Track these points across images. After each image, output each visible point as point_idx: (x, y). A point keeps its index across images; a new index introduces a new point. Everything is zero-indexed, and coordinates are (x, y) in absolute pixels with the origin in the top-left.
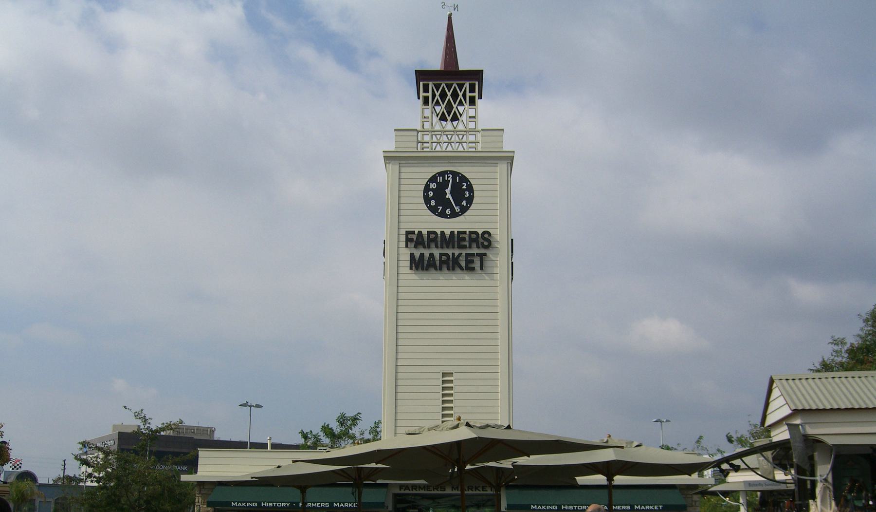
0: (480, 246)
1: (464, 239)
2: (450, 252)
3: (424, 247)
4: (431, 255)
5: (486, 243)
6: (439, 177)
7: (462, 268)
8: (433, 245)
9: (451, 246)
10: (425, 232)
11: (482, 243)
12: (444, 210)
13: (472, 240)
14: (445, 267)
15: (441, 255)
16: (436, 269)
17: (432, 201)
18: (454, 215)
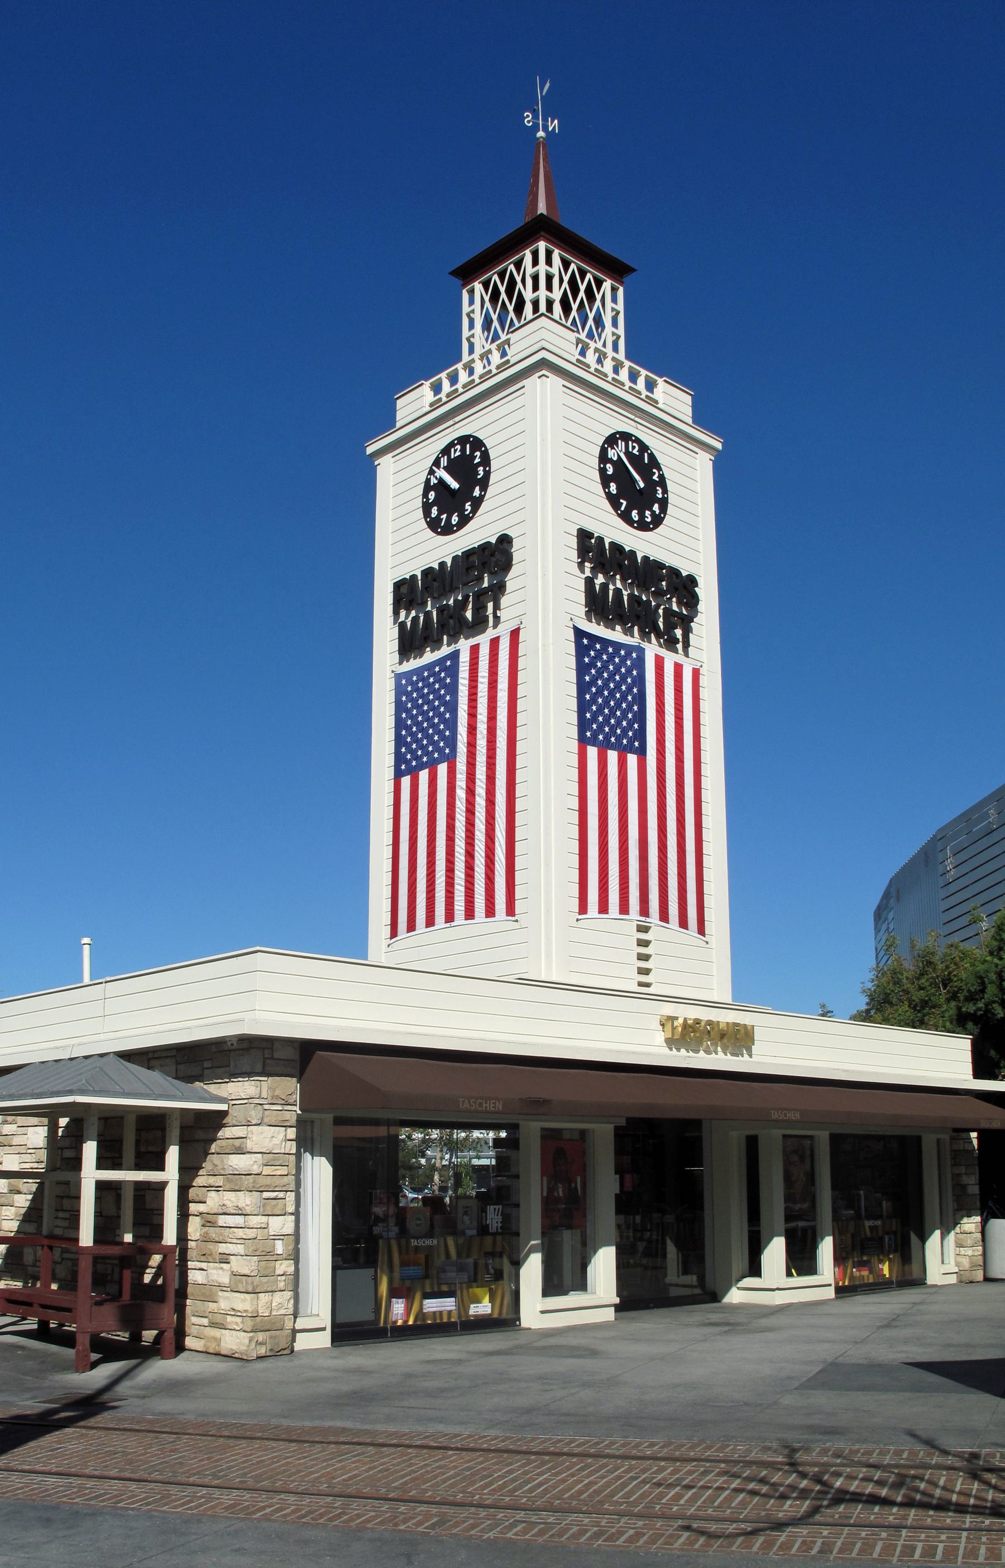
6: (442, 459)
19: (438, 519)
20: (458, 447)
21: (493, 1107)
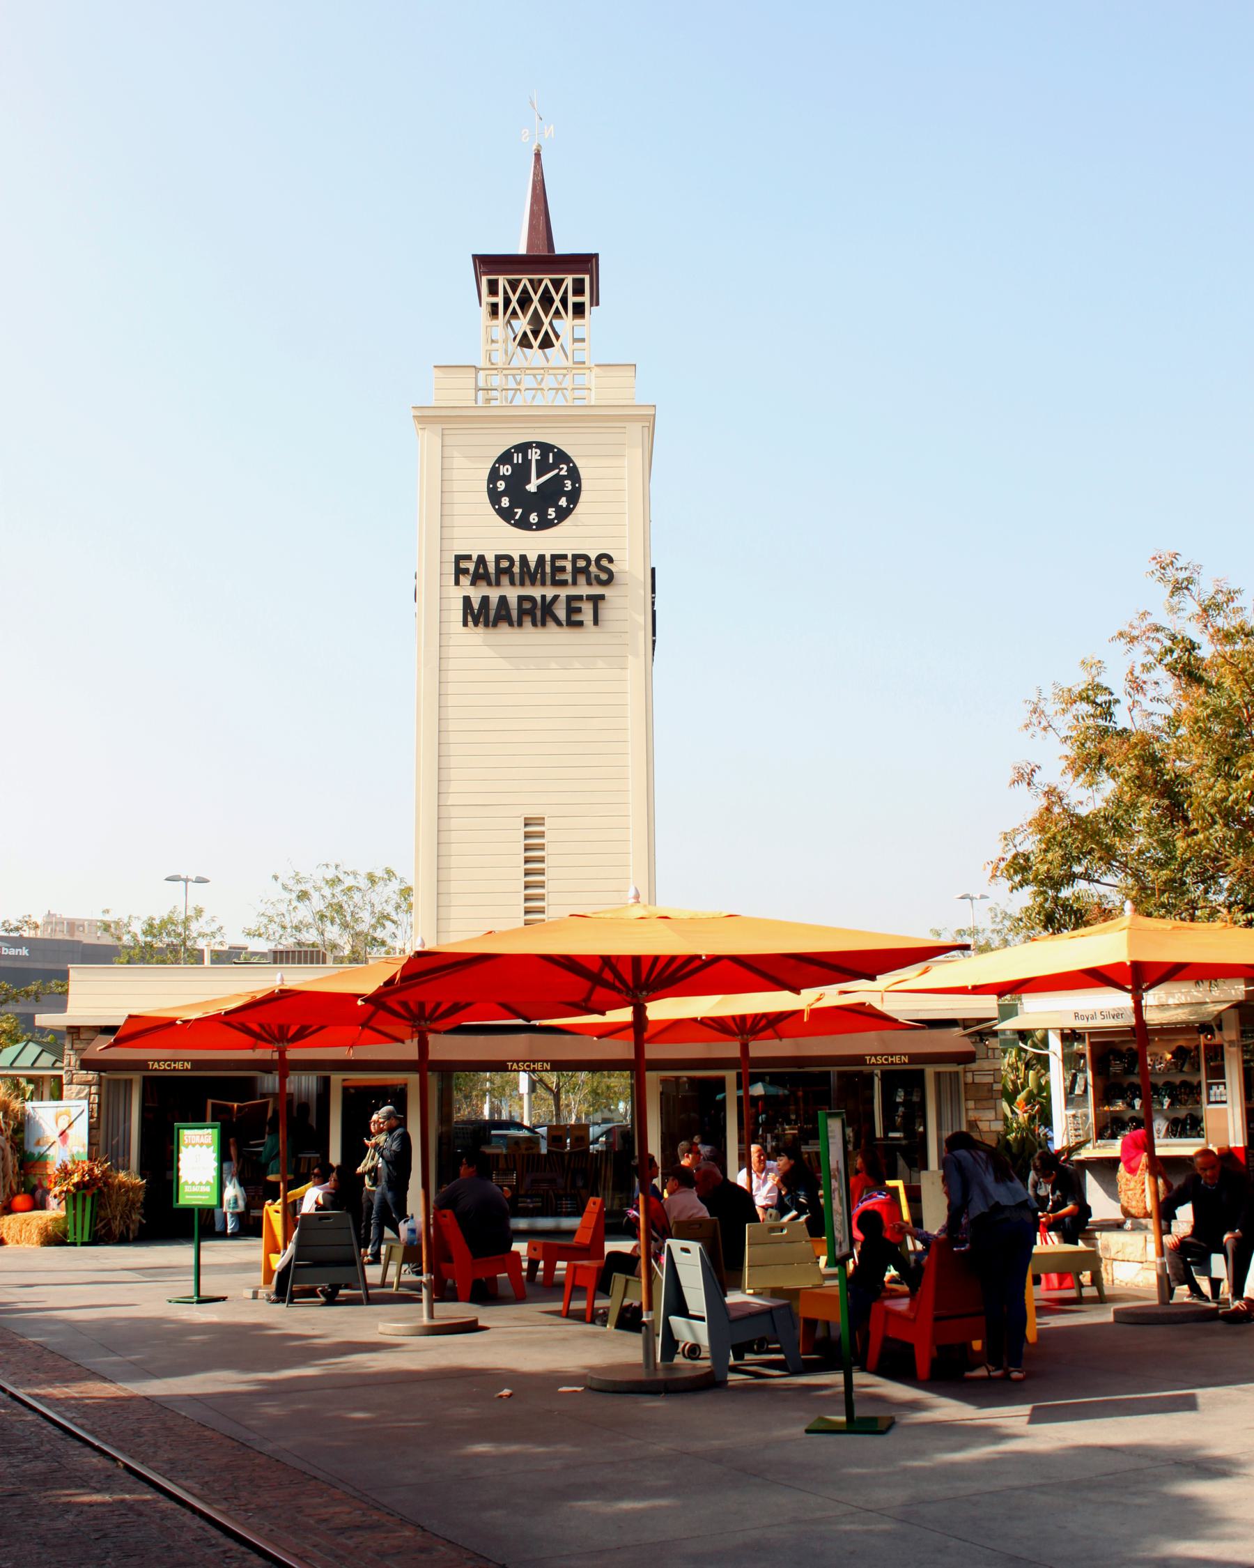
0: (594, 582)
1: (563, 569)
2: (536, 592)
3: (490, 584)
4: (503, 600)
5: (604, 577)
6: (515, 455)
7: (559, 623)
8: (505, 580)
9: (538, 582)
10: (490, 559)
11: (597, 577)
12: (525, 516)
13: (576, 571)
14: (527, 621)
15: (521, 599)
16: (511, 624)
17: (503, 499)
18: (545, 524)
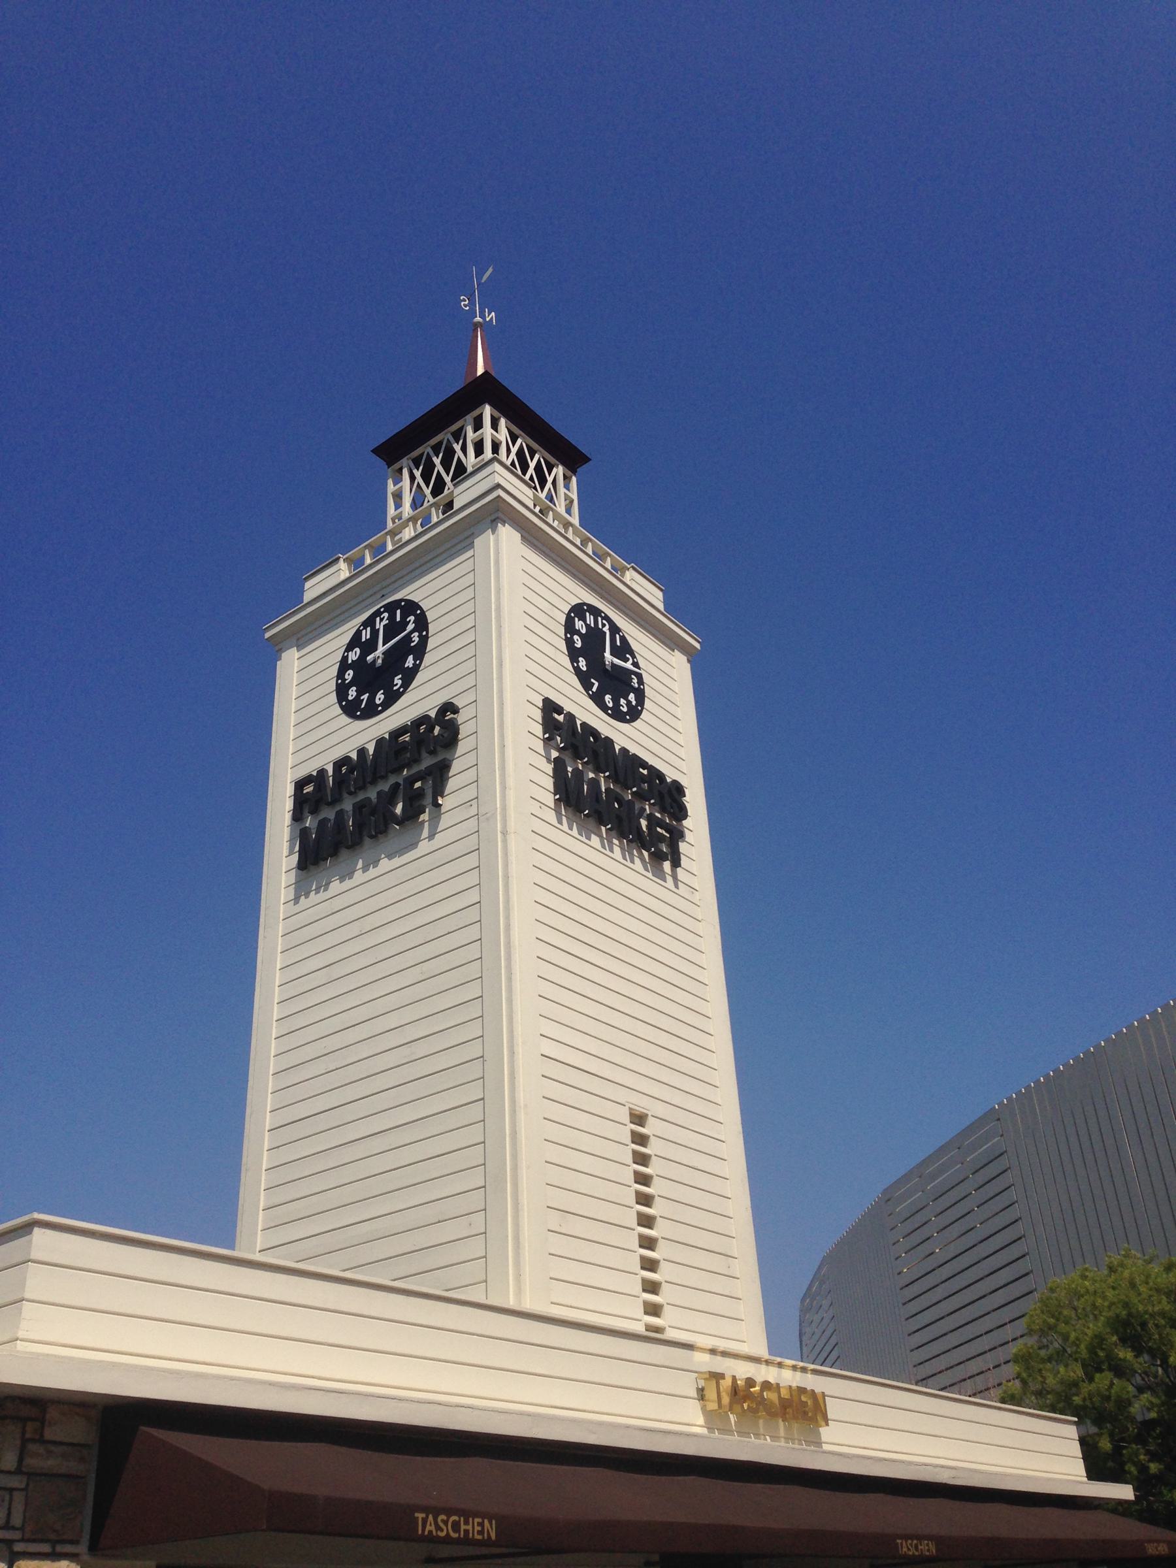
6: (364, 632)
12: (371, 699)
19: (358, 700)
20: (386, 615)
21: (479, 1533)
